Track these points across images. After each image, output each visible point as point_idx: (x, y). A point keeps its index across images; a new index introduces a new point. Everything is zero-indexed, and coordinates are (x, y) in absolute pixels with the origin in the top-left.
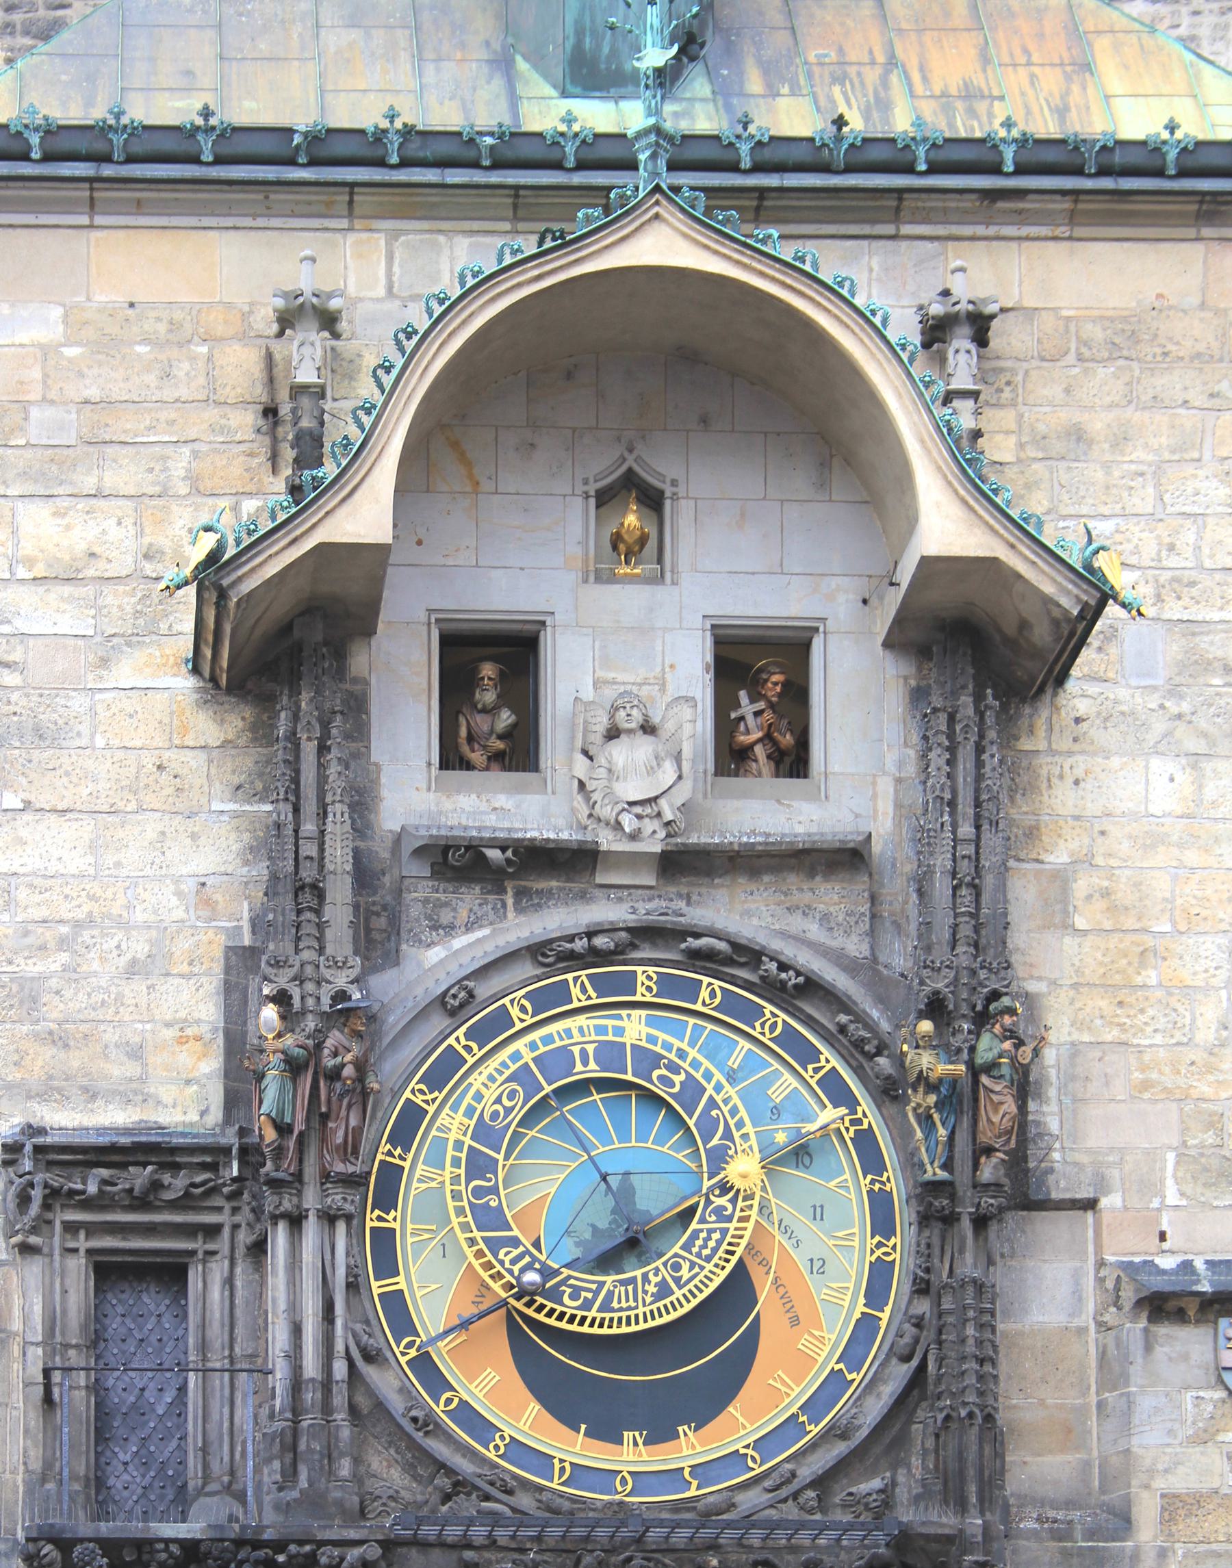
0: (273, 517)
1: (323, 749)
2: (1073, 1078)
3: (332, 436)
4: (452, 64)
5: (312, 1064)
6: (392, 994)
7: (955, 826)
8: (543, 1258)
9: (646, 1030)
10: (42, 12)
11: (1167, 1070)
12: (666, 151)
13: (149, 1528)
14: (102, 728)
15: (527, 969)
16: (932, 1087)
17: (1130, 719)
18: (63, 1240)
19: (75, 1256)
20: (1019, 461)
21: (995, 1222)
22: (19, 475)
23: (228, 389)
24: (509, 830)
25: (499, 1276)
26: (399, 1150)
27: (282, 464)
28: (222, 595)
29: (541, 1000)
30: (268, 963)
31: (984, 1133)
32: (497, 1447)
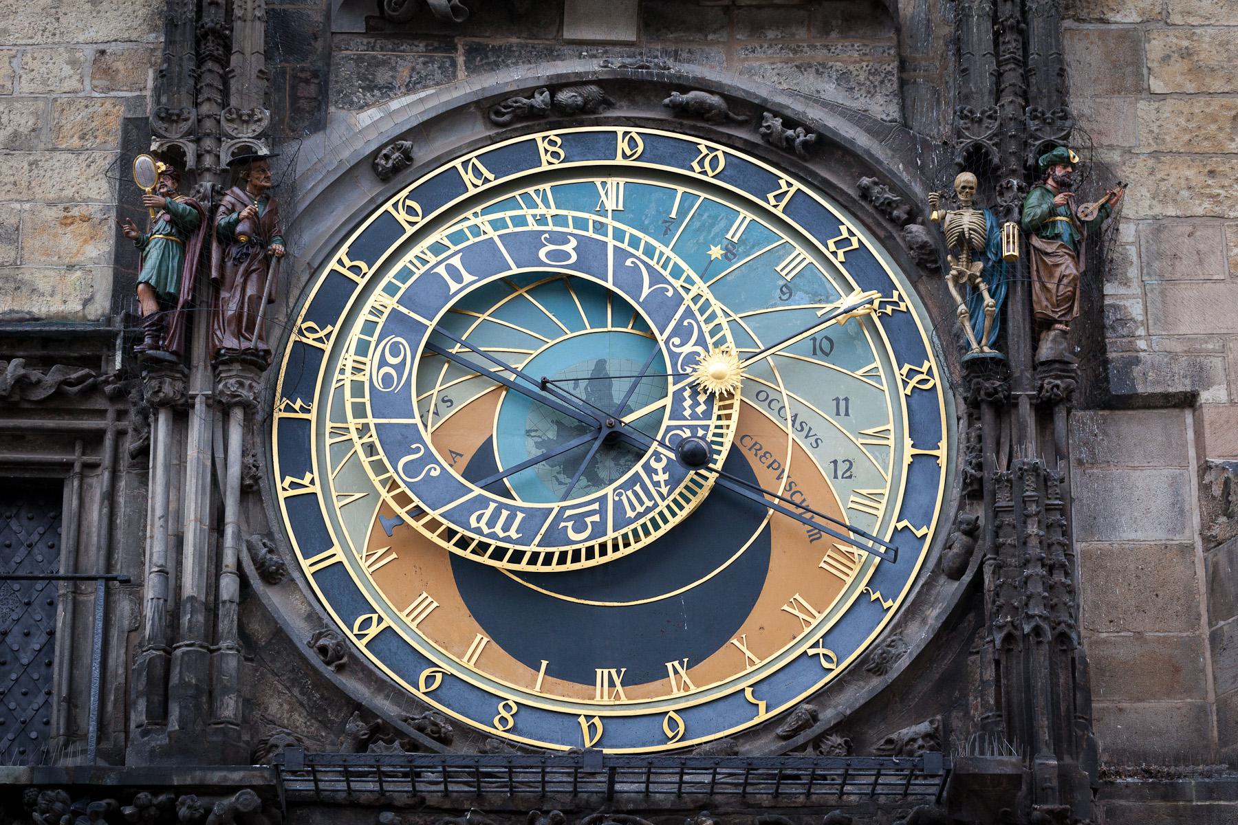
5: (204, 225)
15: (480, 130)
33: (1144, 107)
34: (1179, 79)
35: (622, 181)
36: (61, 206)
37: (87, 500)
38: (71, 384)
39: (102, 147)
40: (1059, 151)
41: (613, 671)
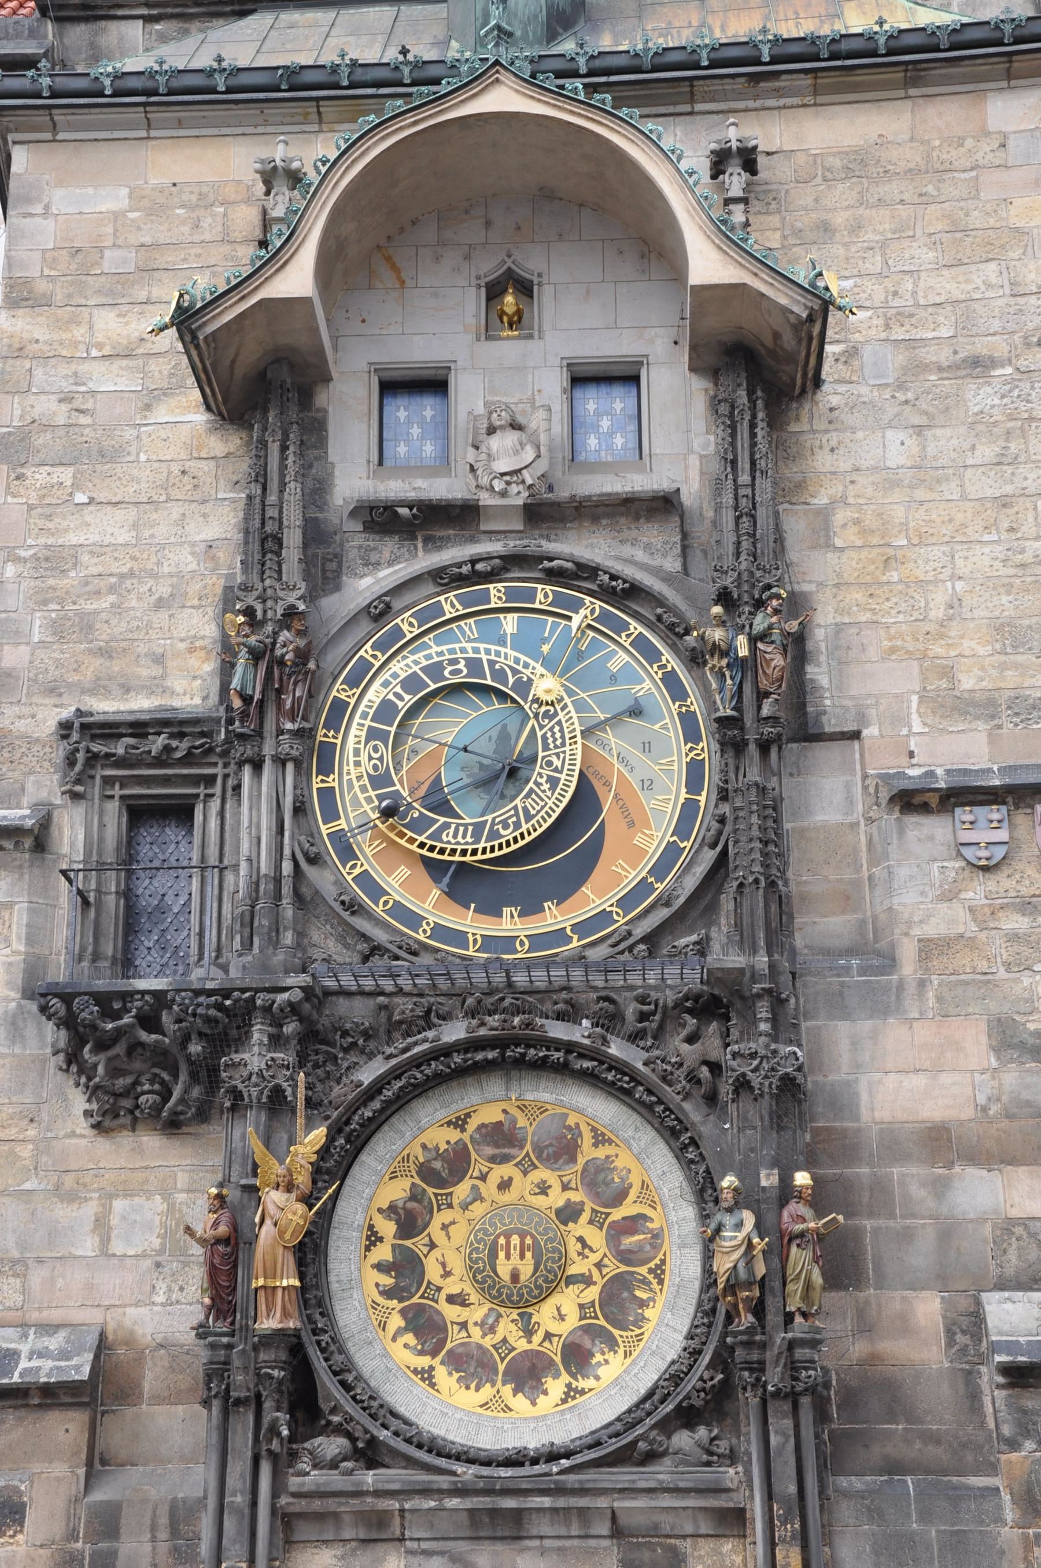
1: (284, 448)
11: (909, 639)
15: (432, 589)
34: (852, 538)
35: (516, 615)
38: (196, 748)
40: (774, 590)
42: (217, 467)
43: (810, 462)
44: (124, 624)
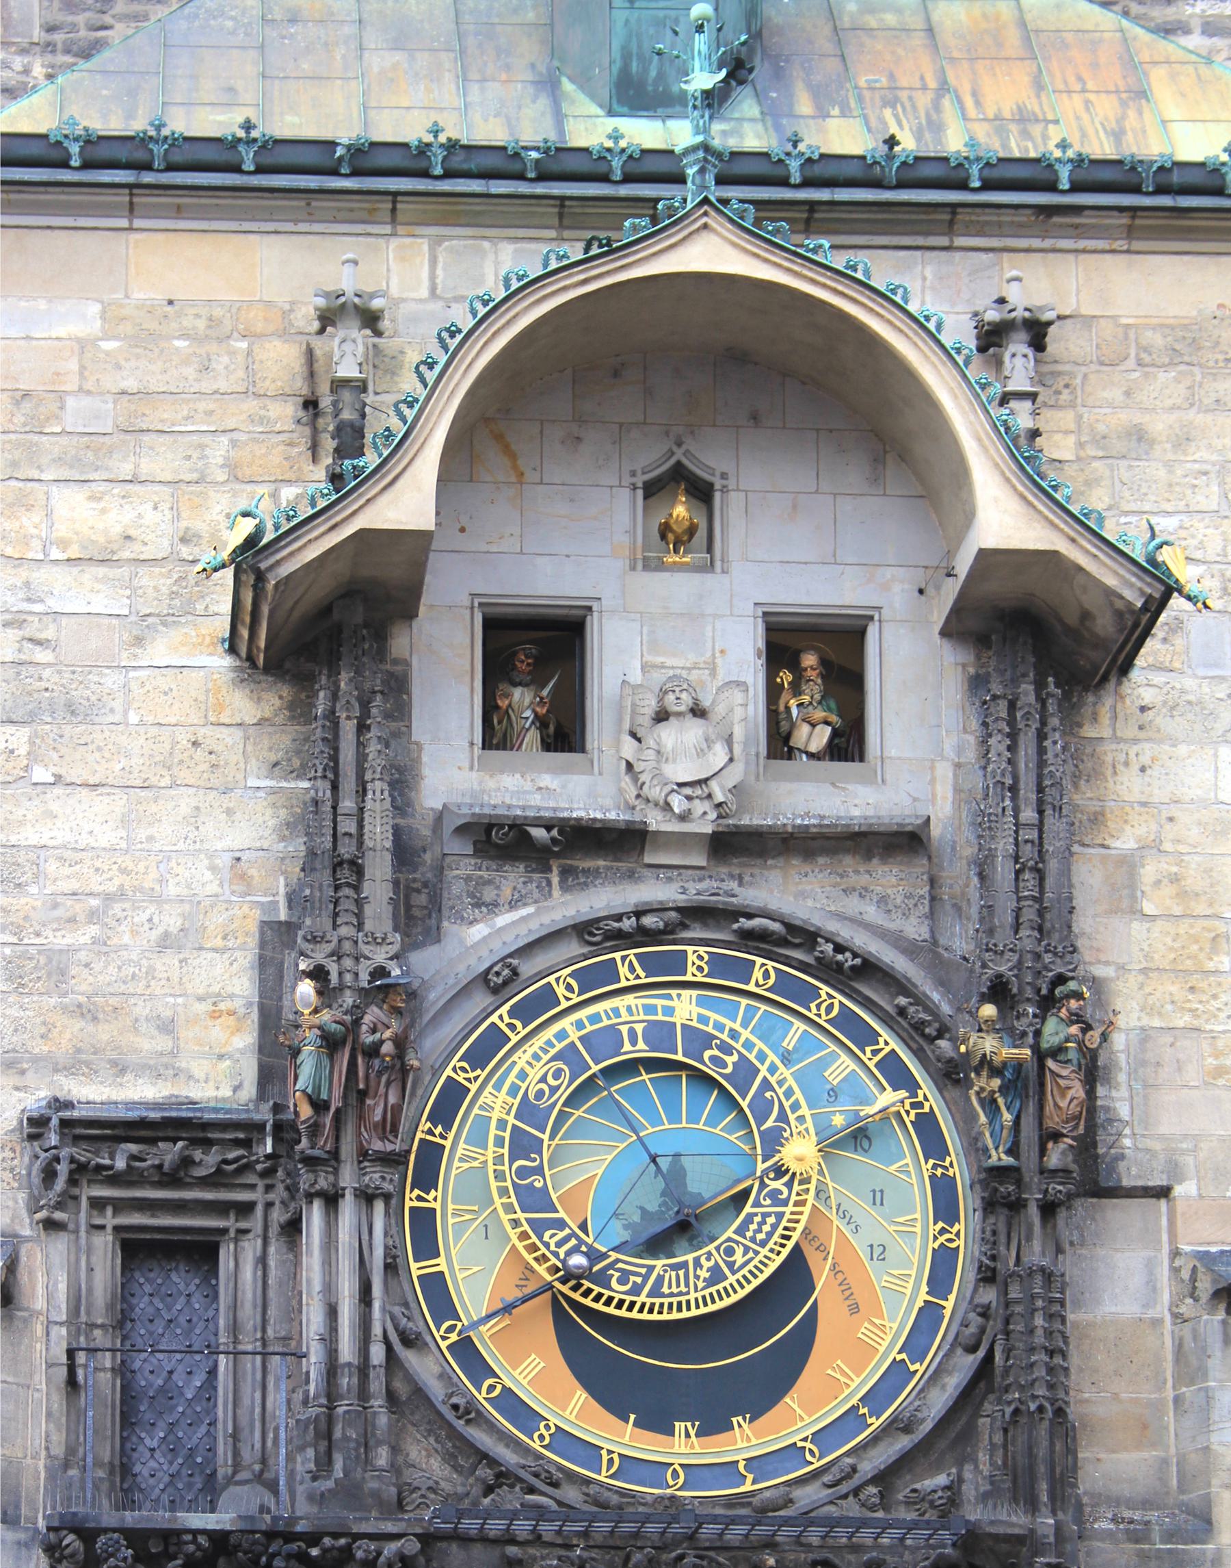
0: (313, 504)
2: (1144, 1063)
3: (373, 427)
4: (497, 85)
5: (350, 1039)
6: (432, 971)
7: (1016, 811)
8: (590, 1241)
9: (697, 1010)
10: (83, 33)
12: (715, 166)
13: (175, 1519)
14: (136, 705)
15: (574, 948)
16: (996, 1071)
17: (1197, 709)
18: (90, 1216)
19: (102, 1233)
20: (1079, 459)
21: (1063, 1209)
22: (54, 460)
23: (268, 382)
24: (555, 810)
25: (545, 1258)
26: (439, 1129)
27: (322, 453)
28: (260, 577)
29: (587, 979)
30: (305, 938)
31: (1052, 1118)
32: (542, 1437)
33: (1137, 928)
34: (1168, 902)
36: (210, 1001)
37: (241, 1261)
39: (242, 947)
41: (689, 1424)
42: (247, 738)
43: (1110, 785)
44: (112, 969)
